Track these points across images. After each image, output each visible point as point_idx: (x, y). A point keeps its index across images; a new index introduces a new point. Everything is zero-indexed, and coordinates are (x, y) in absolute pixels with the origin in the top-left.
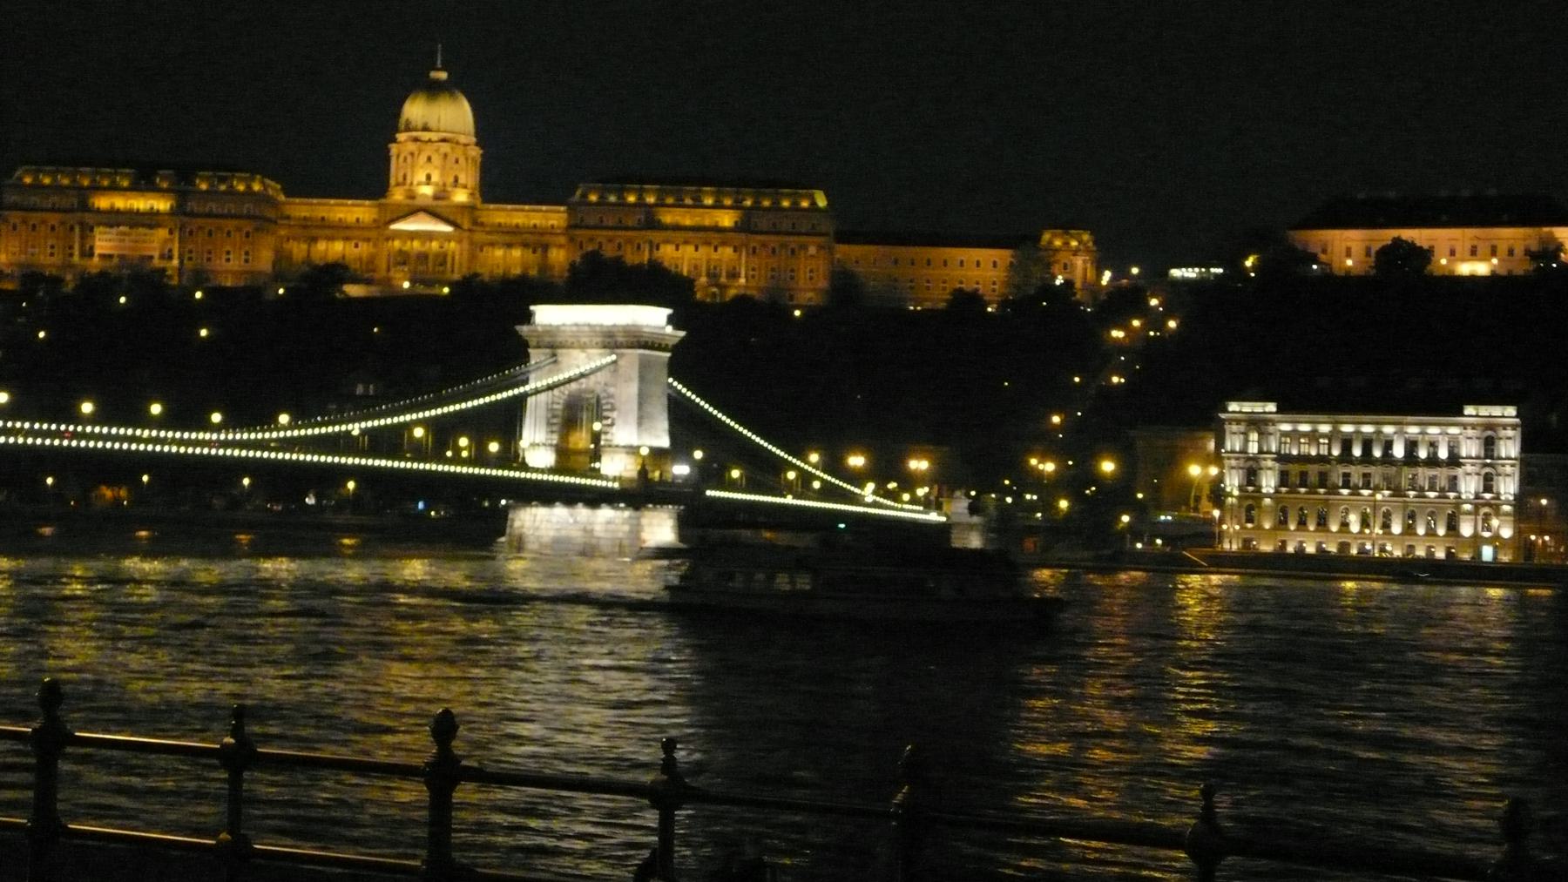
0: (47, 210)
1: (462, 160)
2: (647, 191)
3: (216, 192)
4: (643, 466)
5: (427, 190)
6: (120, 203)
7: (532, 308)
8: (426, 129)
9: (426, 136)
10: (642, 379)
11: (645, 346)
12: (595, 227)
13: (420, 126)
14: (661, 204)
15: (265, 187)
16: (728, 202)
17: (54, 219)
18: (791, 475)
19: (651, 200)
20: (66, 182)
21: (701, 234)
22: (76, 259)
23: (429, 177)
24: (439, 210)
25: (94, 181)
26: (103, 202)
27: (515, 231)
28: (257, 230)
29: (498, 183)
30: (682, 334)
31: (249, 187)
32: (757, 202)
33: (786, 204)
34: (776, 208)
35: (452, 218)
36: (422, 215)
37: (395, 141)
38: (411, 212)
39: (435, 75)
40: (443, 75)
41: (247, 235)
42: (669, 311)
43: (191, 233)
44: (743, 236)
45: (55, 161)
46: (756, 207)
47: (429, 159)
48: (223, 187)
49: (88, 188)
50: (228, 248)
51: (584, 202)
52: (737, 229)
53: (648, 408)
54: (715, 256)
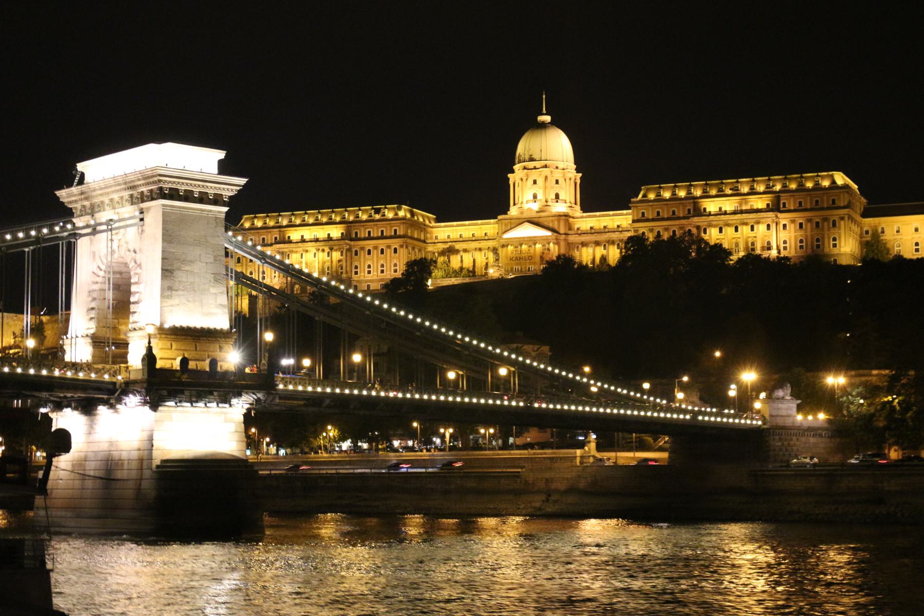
1: (561, 181)
2: (695, 186)
3: (373, 221)
4: (150, 349)
5: (536, 207)
6: (309, 233)
7: (81, 167)
8: (532, 159)
9: (531, 164)
10: (168, 237)
11: (173, 195)
12: (653, 220)
13: (527, 158)
14: (706, 196)
15: (413, 214)
16: (762, 188)
18: (503, 371)
19: (698, 193)
20: (271, 223)
21: (738, 216)
23: (535, 197)
24: (541, 220)
26: (295, 235)
28: (402, 246)
29: (593, 197)
30: (242, 181)
31: (396, 214)
32: (784, 186)
33: (809, 185)
34: (801, 188)
35: (551, 225)
36: (527, 225)
37: (513, 172)
38: (520, 222)
40: (547, 119)
41: (395, 251)
42: (221, 154)
43: (356, 252)
44: (771, 214)
46: (785, 190)
47: (535, 182)
48: (377, 217)
49: (287, 226)
50: (382, 262)
51: (645, 200)
52: (768, 209)
53: (180, 276)
54: (752, 234)
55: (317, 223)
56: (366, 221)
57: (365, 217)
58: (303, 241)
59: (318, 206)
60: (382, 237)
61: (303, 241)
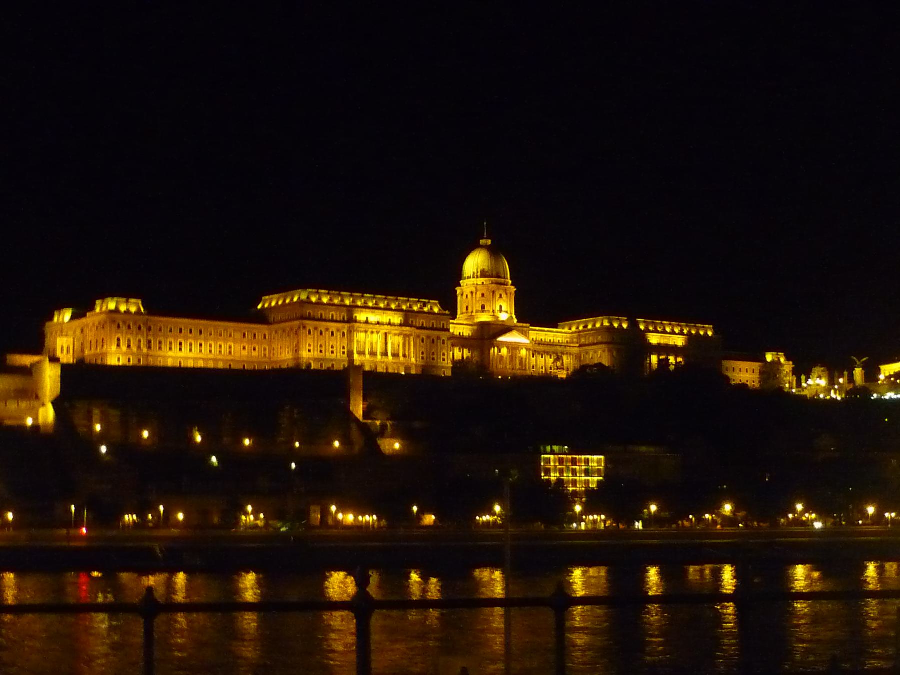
0: (329, 321)
3: (425, 313)
6: (374, 317)
8: (499, 277)
16: (677, 330)
17: (333, 326)
20: (336, 301)
22: (356, 356)
23: (501, 307)
25: (354, 302)
26: (361, 316)
27: (551, 344)
36: (514, 332)
39: (482, 242)
40: (489, 242)
45: (334, 286)
48: (426, 309)
55: (376, 308)
56: (418, 312)
57: (415, 309)
58: (367, 322)
59: (375, 292)
60: (433, 329)
61: (367, 322)
